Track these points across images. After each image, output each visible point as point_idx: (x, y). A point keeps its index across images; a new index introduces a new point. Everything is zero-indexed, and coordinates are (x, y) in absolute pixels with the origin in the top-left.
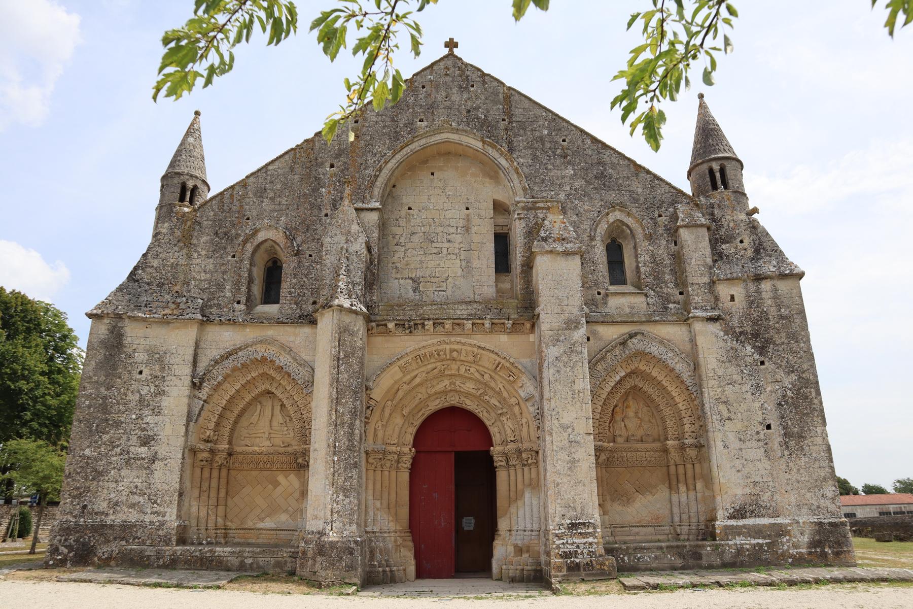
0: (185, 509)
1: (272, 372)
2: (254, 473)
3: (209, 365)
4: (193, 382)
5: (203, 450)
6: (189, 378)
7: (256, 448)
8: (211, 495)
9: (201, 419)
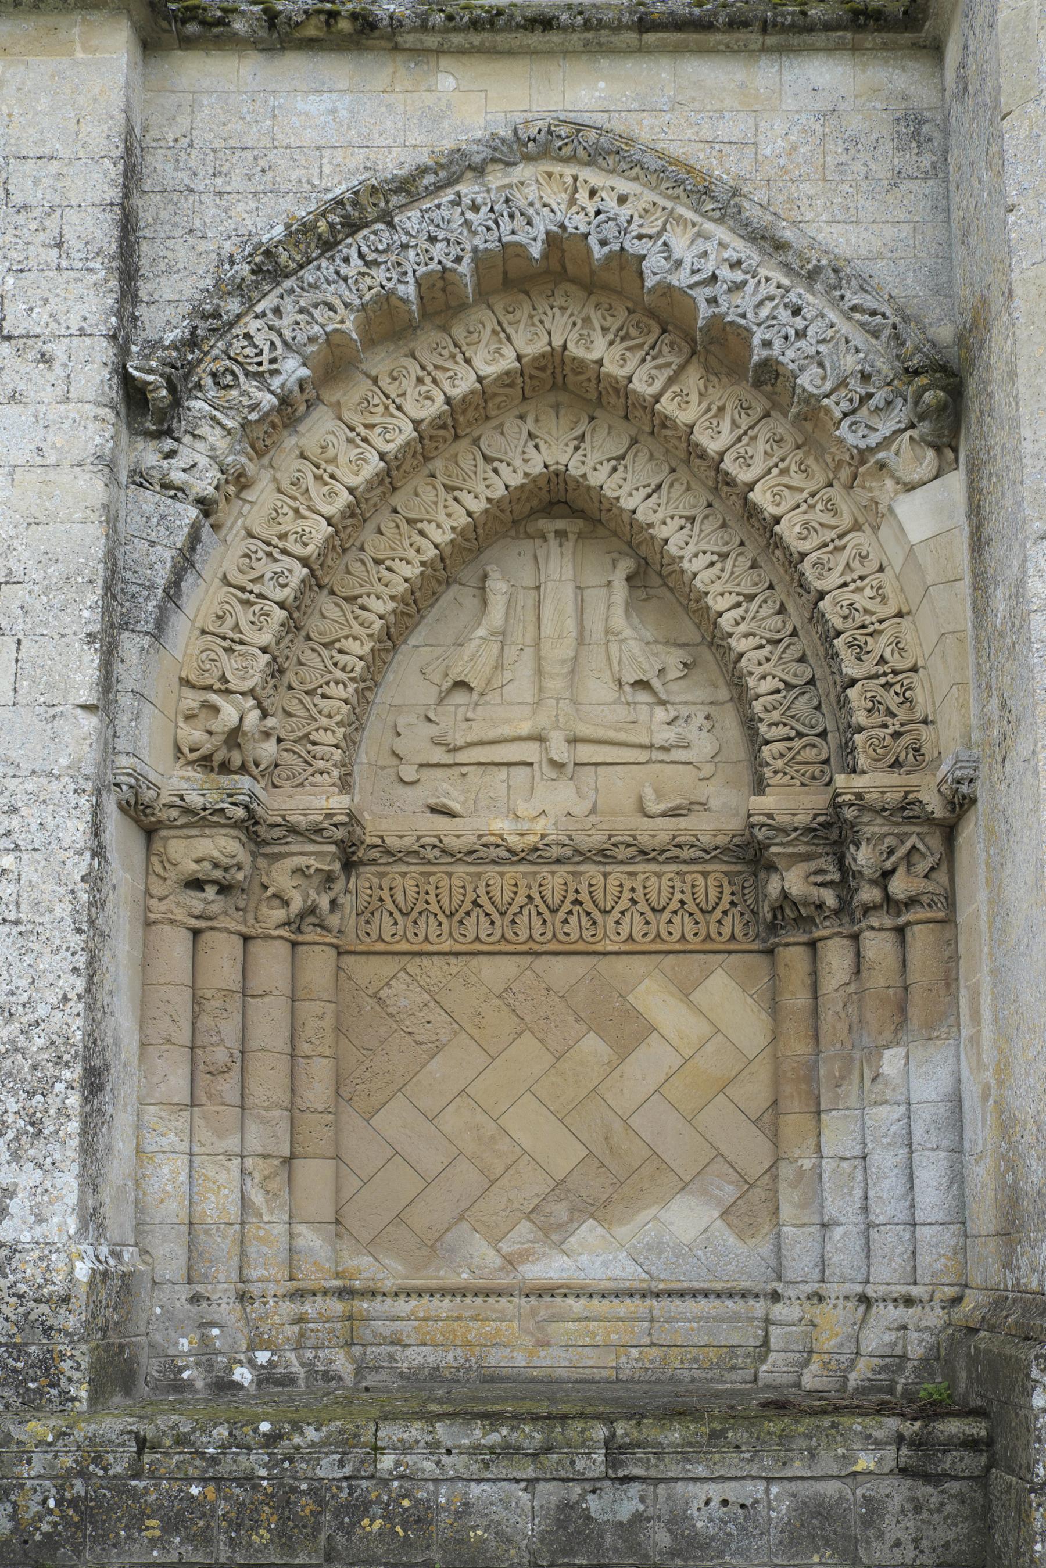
0: (117, 1169)
1: (600, 350)
2: (496, 971)
3: (222, 288)
4: (126, 380)
5: (199, 819)
6: (104, 351)
7: (501, 825)
8: (258, 1093)
9: (181, 629)
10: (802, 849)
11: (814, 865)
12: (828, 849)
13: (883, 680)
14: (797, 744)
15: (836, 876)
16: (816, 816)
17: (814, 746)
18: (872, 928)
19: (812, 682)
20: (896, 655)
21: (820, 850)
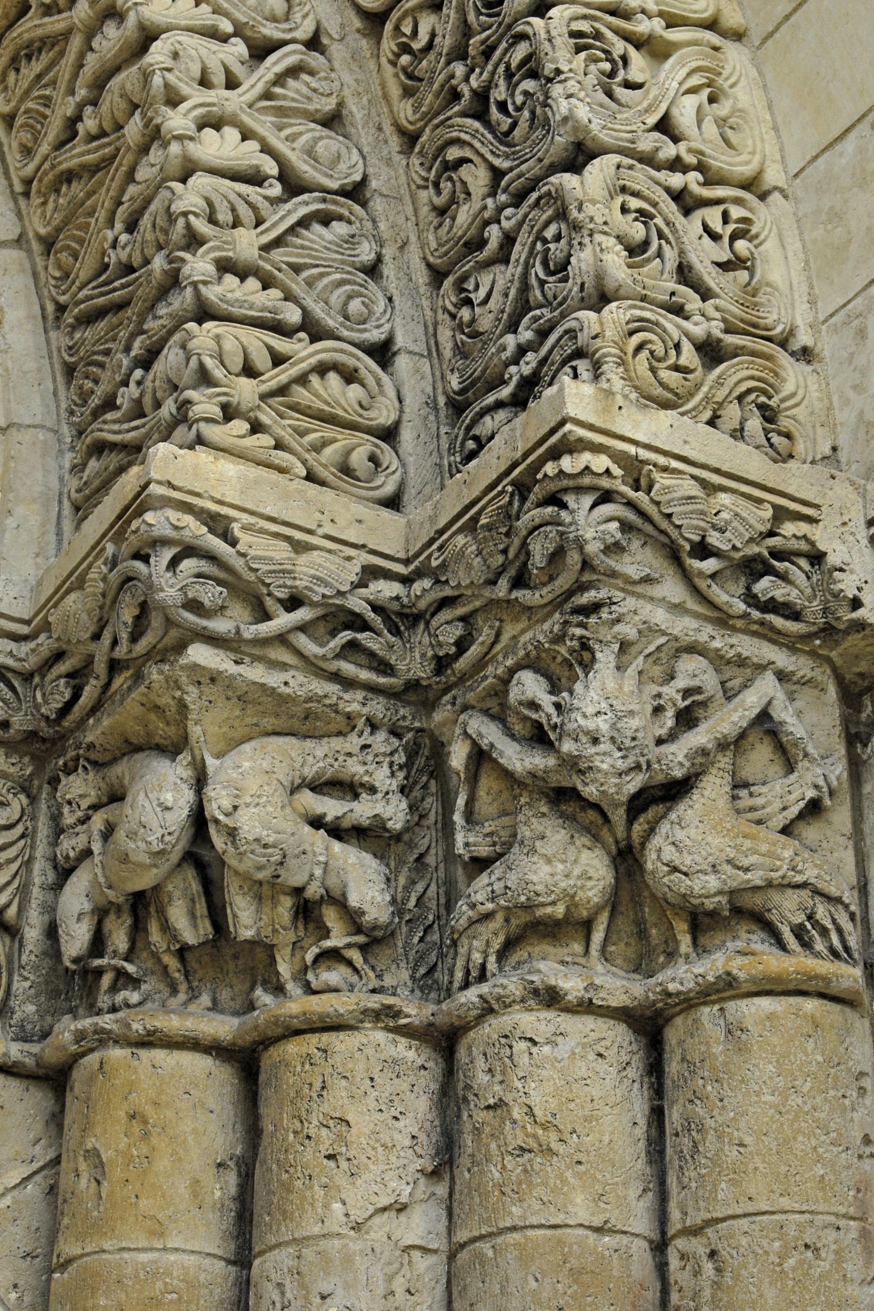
10: (297, 683)
11: (318, 756)
12: (377, 707)
13: (676, 180)
14: (304, 352)
15: (395, 812)
16: (370, 573)
17: (350, 377)
18: (551, 998)
19: (356, 192)
20: (710, 129)
21: (353, 702)
